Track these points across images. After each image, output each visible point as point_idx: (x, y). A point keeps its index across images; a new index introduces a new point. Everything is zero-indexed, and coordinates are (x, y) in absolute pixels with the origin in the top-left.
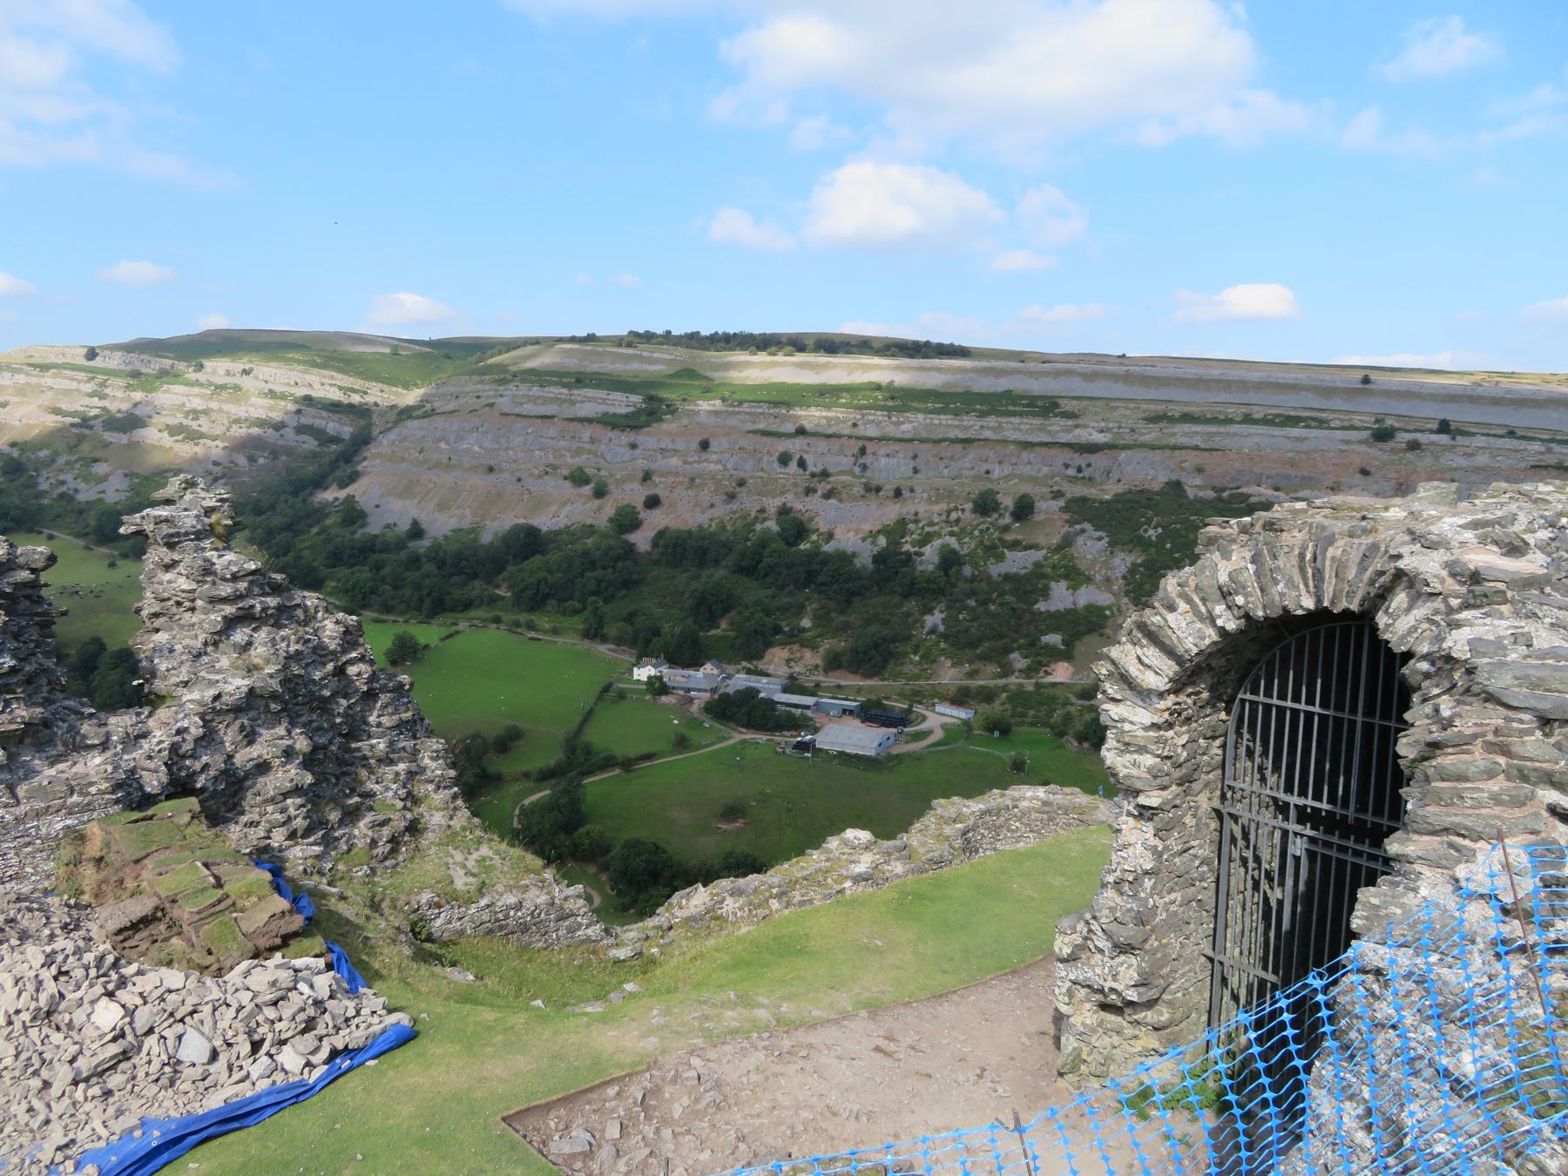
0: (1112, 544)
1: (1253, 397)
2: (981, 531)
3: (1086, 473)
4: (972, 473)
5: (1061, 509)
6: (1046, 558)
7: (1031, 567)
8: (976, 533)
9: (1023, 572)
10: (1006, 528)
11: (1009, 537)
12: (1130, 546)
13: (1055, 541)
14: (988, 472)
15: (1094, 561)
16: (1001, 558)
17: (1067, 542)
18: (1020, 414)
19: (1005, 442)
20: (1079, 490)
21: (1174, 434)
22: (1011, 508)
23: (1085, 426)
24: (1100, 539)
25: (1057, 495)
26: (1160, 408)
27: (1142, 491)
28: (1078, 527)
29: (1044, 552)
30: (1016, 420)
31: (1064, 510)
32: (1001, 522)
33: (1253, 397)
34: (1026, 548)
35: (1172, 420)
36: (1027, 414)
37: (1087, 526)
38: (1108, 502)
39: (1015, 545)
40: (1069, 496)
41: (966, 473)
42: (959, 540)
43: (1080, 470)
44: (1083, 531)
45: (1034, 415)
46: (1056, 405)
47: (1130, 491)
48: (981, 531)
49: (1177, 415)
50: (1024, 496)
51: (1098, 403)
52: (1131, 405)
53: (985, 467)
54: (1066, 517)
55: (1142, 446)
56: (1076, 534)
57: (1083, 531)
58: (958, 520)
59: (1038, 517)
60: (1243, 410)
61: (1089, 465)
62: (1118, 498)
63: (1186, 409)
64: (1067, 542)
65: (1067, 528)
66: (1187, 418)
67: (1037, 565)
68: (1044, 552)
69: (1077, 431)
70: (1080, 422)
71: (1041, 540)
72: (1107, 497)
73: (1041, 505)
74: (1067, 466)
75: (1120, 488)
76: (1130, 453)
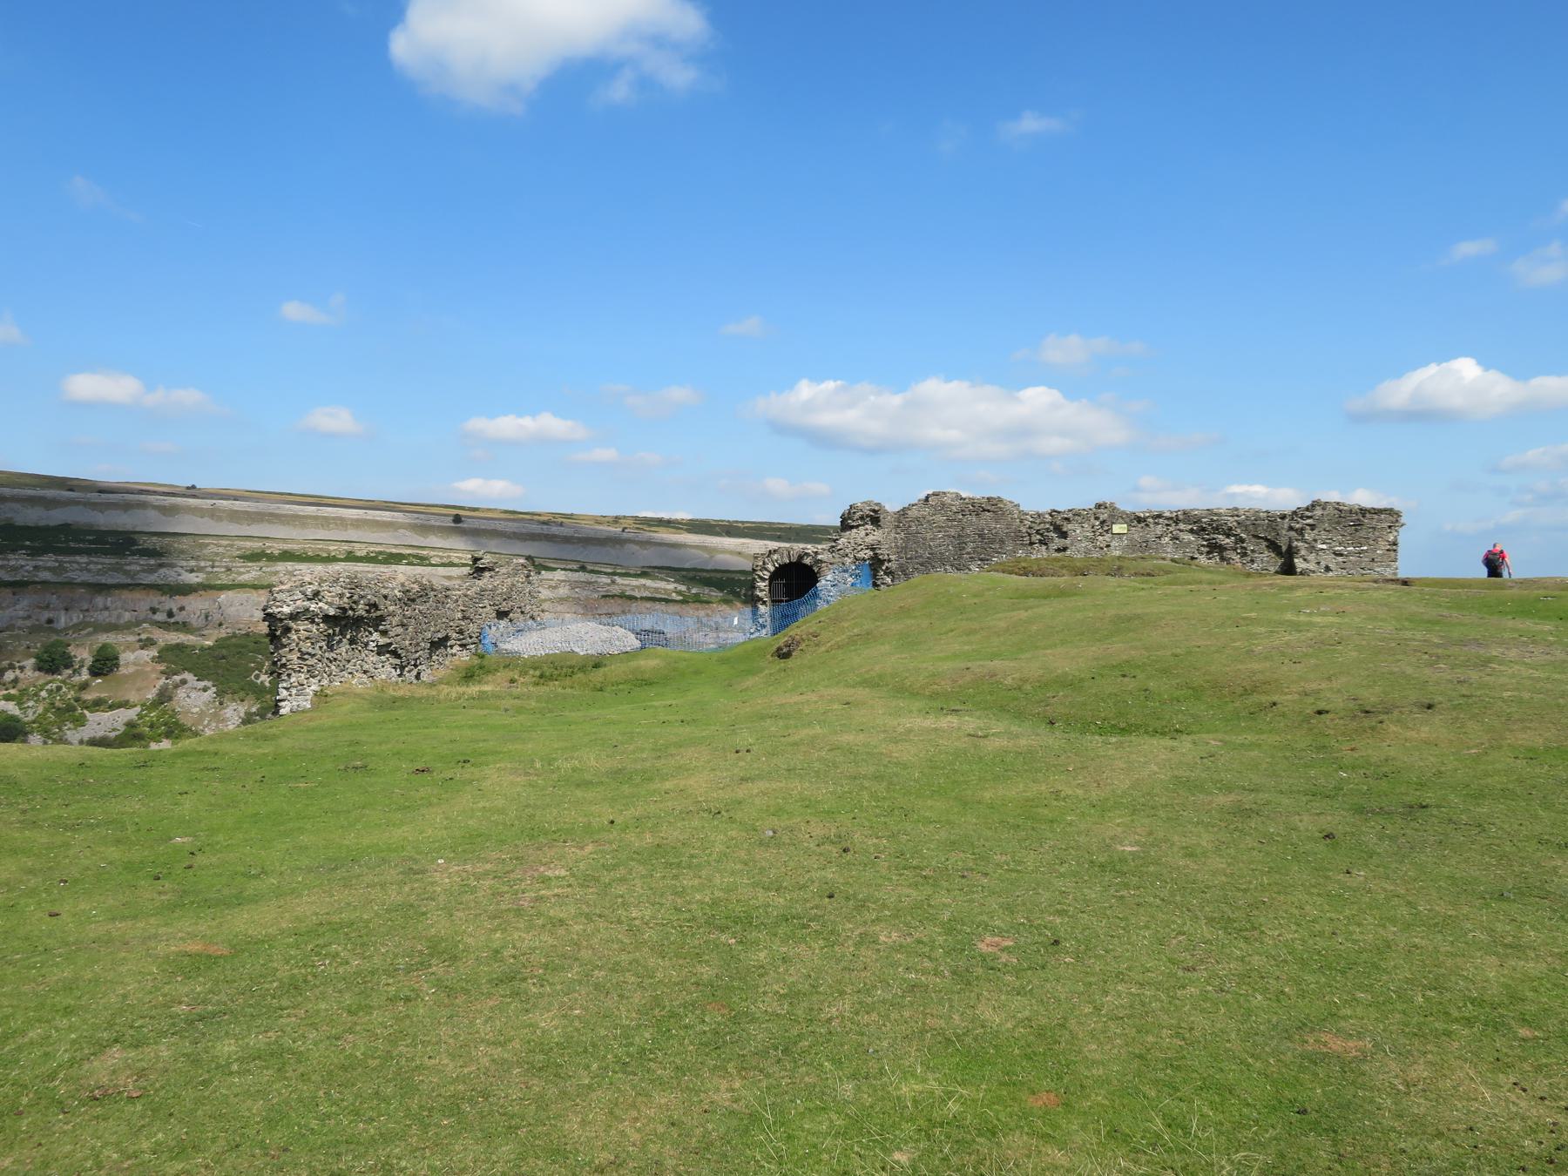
0: (220, 694)
1: (352, 534)
2: (50, 692)
3: (179, 618)
4: (28, 623)
5: (153, 659)
6: (140, 716)
7: (122, 729)
8: (44, 694)
9: (113, 735)
10: (84, 686)
11: (89, 696)
12: (242, 694)
13: (151, 695)
14: (50, 621)
15: (202, 714)
16: (80, 722)
17: (164, 697)
18: (88, 552)
19: (70, 584)
20: (175, 638)
21: (276, 573)
22: (89, 661)
23: (172, 566)
24: (205, 689)
25: (147, 644)
26: (257, 545)
27: (247, 635)
28: (177, 678)
29: (138, 709)
30: (83, 559)
31: (159, 659)
32: (76, 679)
33: (352, 534)
34: (111, 708)
35: (271, 558)
36: (95, 552)
37: (188, 676)
38: (210, 648)
39: (97, 705)
40: (161, 643)
41: (20, 623)
42: (19, 704)
43: (170, 614)
44: (184, 682)
45: (106, 553)
46: (134, 543)
47: (234, 635)
48: (50, 692)
49: (276, 552)
50: (104, 647)
51: (184, 539)
52: (225, 542)
53: (46, 615)
54: (162, 667)
55: (242, 586)
56: (176, 686)
57: (184, 682)
58: (16, 681)
59: (123, 671)
60: (346, 547)
61: (182, 609)
62: (221, 643)
63: (287, 547)
64: (164, 697)
65: (163, 681)
66: (287, 556)
67: (130, 725)
68: (138, 709)
69: (162, 571)
70: (163, 560)
71: (133, 697)
72: (209, 643)
73: (127, 657)
74: (154, 611)
75: (223, 633)
76: (230, 593)
